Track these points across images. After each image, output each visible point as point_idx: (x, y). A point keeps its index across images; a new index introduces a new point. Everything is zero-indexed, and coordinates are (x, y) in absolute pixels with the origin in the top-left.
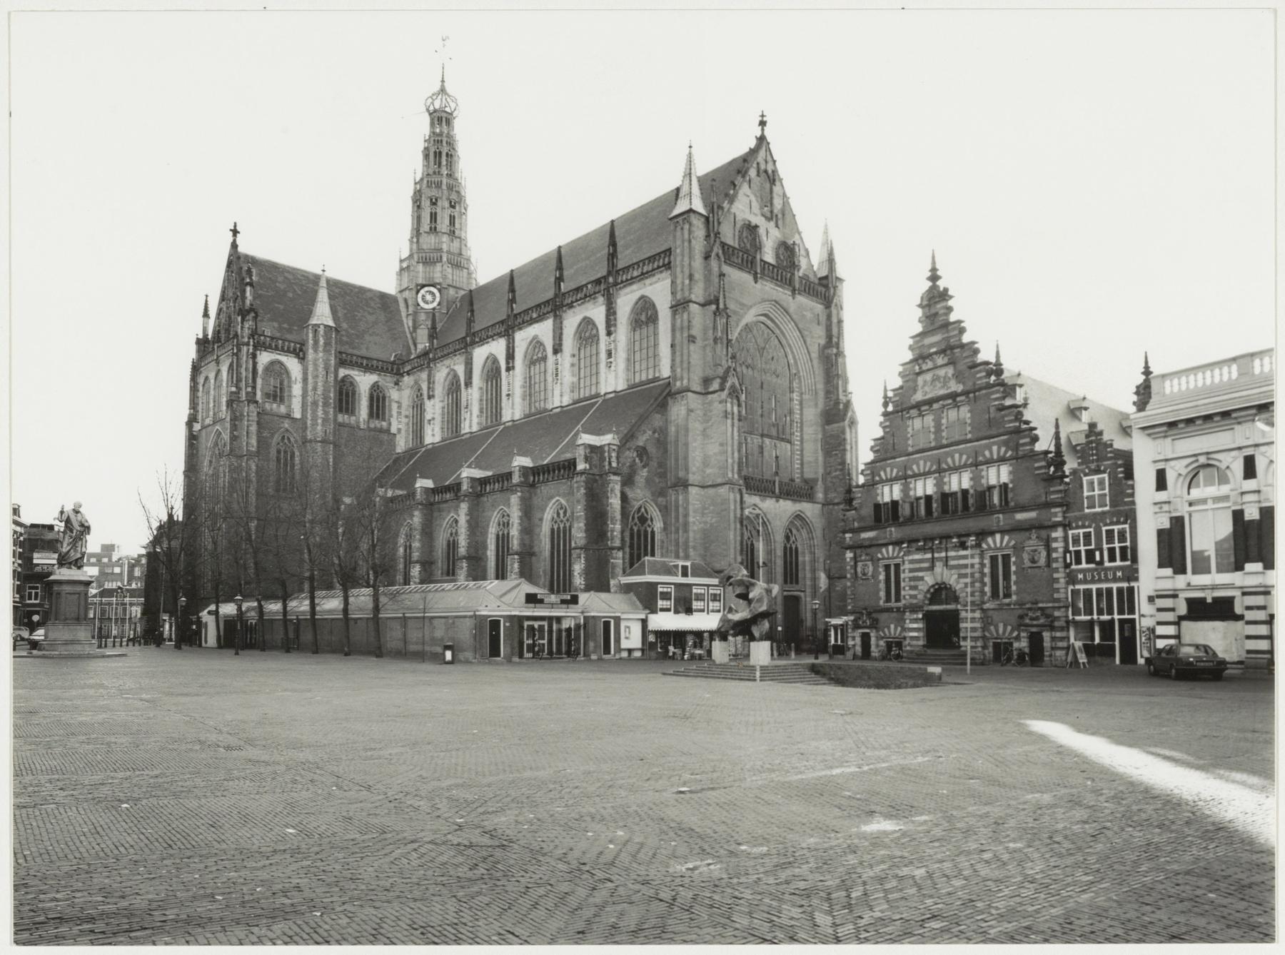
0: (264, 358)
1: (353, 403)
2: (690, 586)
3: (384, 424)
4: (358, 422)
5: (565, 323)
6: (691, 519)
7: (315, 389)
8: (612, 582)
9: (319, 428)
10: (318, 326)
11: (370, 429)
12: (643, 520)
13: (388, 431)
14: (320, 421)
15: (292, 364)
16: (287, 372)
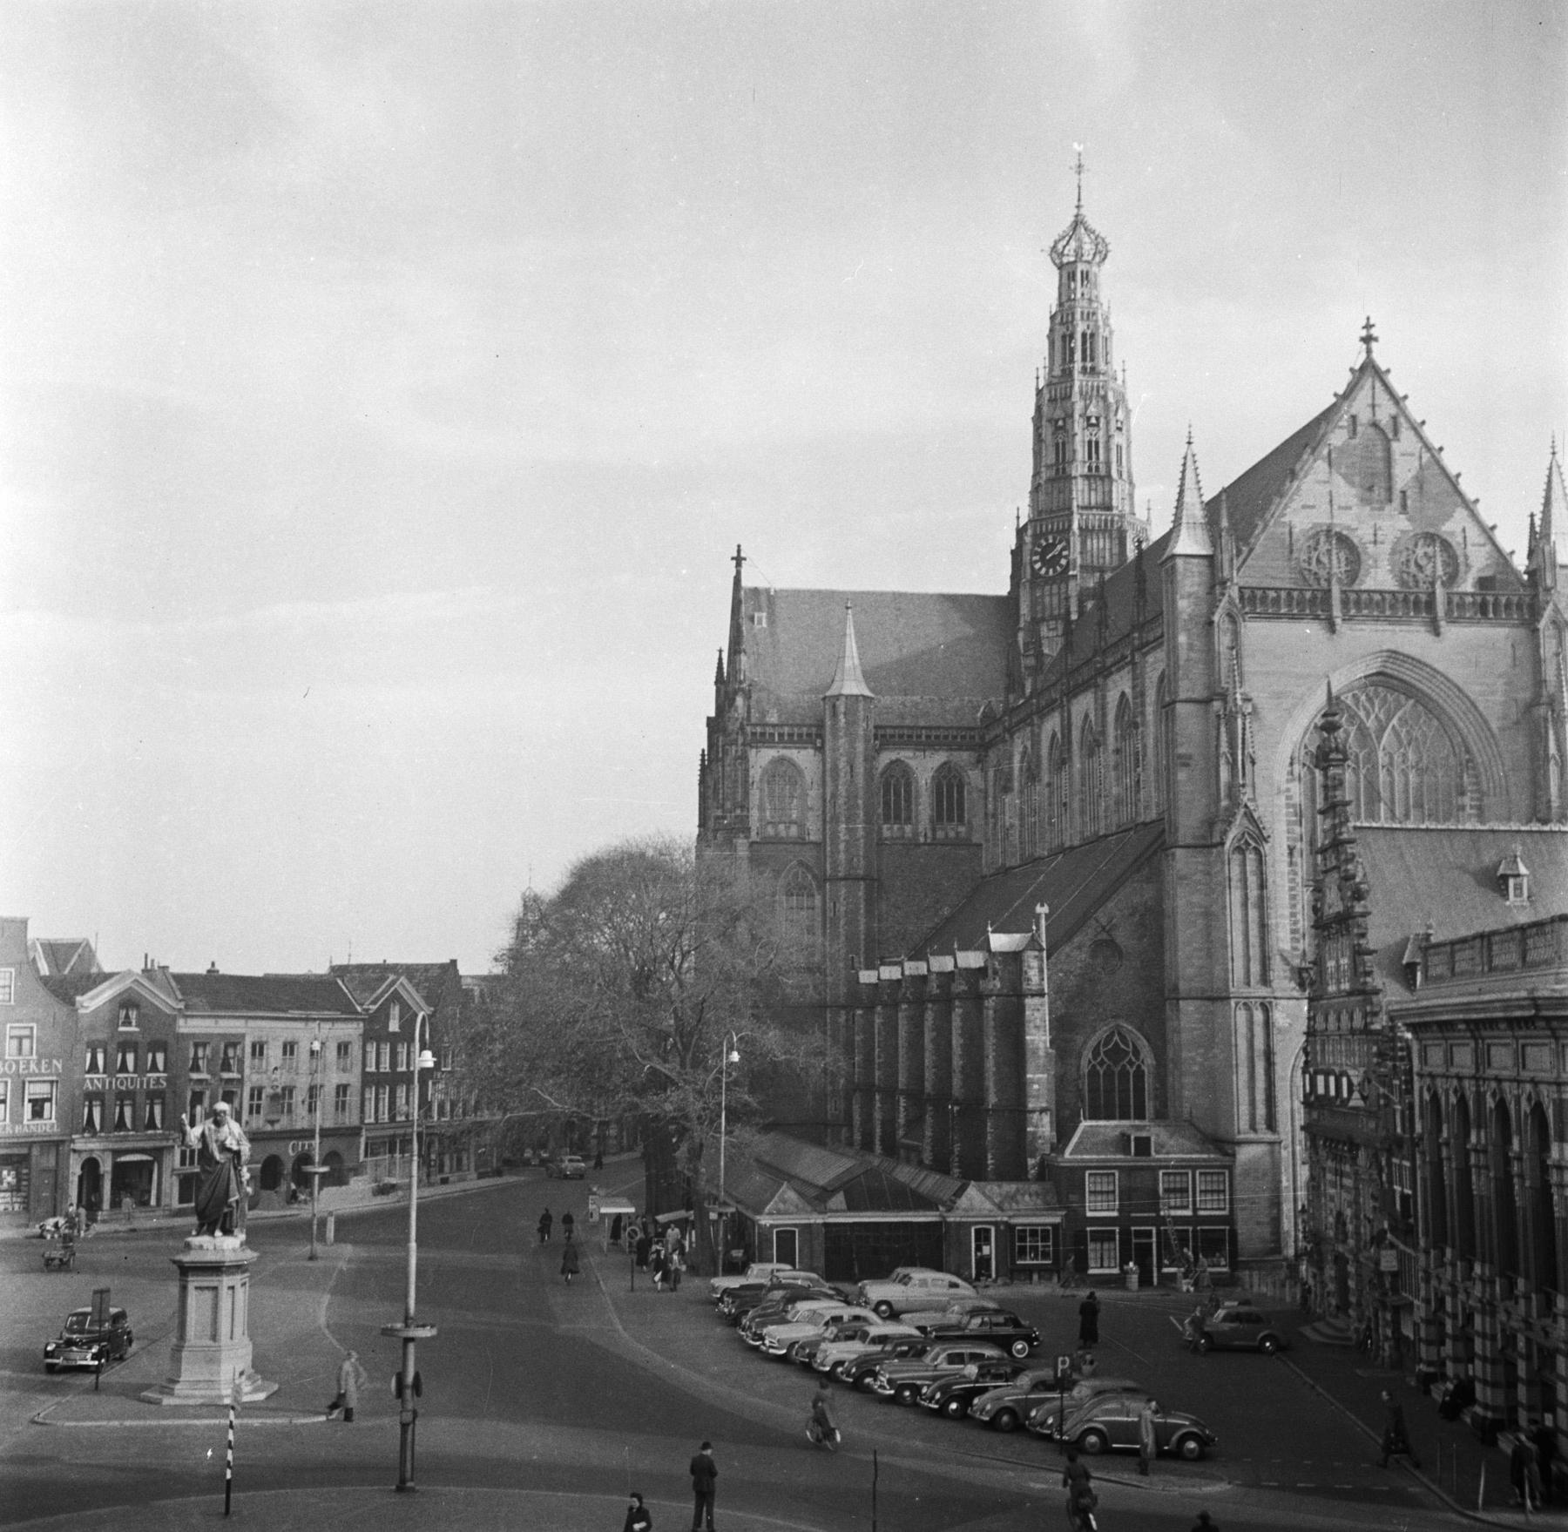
0: (760, 758)
1: (908, 801)
2: (1154, 1170)
3: (962, 829)
4: (916, 834)
5: (1109, 699)
6: (1184, 1054)
7: (834, 796)
8: (1031, 1162)
9: (842, 856)
10: (838, 697)
11: (935, 843)
12: (1116, 1054)
13: (966, 843)
14: (842, 846)
15: (804, 758)
16: (800, 772)
